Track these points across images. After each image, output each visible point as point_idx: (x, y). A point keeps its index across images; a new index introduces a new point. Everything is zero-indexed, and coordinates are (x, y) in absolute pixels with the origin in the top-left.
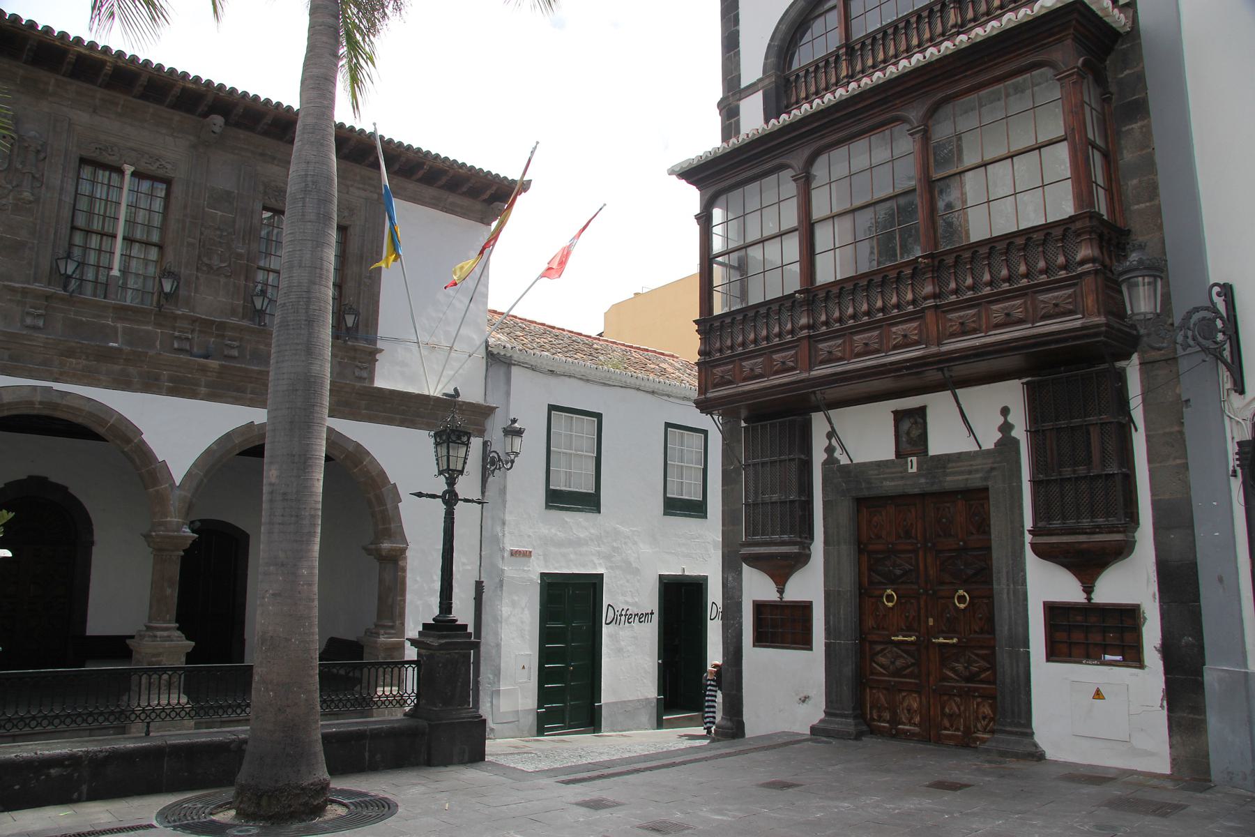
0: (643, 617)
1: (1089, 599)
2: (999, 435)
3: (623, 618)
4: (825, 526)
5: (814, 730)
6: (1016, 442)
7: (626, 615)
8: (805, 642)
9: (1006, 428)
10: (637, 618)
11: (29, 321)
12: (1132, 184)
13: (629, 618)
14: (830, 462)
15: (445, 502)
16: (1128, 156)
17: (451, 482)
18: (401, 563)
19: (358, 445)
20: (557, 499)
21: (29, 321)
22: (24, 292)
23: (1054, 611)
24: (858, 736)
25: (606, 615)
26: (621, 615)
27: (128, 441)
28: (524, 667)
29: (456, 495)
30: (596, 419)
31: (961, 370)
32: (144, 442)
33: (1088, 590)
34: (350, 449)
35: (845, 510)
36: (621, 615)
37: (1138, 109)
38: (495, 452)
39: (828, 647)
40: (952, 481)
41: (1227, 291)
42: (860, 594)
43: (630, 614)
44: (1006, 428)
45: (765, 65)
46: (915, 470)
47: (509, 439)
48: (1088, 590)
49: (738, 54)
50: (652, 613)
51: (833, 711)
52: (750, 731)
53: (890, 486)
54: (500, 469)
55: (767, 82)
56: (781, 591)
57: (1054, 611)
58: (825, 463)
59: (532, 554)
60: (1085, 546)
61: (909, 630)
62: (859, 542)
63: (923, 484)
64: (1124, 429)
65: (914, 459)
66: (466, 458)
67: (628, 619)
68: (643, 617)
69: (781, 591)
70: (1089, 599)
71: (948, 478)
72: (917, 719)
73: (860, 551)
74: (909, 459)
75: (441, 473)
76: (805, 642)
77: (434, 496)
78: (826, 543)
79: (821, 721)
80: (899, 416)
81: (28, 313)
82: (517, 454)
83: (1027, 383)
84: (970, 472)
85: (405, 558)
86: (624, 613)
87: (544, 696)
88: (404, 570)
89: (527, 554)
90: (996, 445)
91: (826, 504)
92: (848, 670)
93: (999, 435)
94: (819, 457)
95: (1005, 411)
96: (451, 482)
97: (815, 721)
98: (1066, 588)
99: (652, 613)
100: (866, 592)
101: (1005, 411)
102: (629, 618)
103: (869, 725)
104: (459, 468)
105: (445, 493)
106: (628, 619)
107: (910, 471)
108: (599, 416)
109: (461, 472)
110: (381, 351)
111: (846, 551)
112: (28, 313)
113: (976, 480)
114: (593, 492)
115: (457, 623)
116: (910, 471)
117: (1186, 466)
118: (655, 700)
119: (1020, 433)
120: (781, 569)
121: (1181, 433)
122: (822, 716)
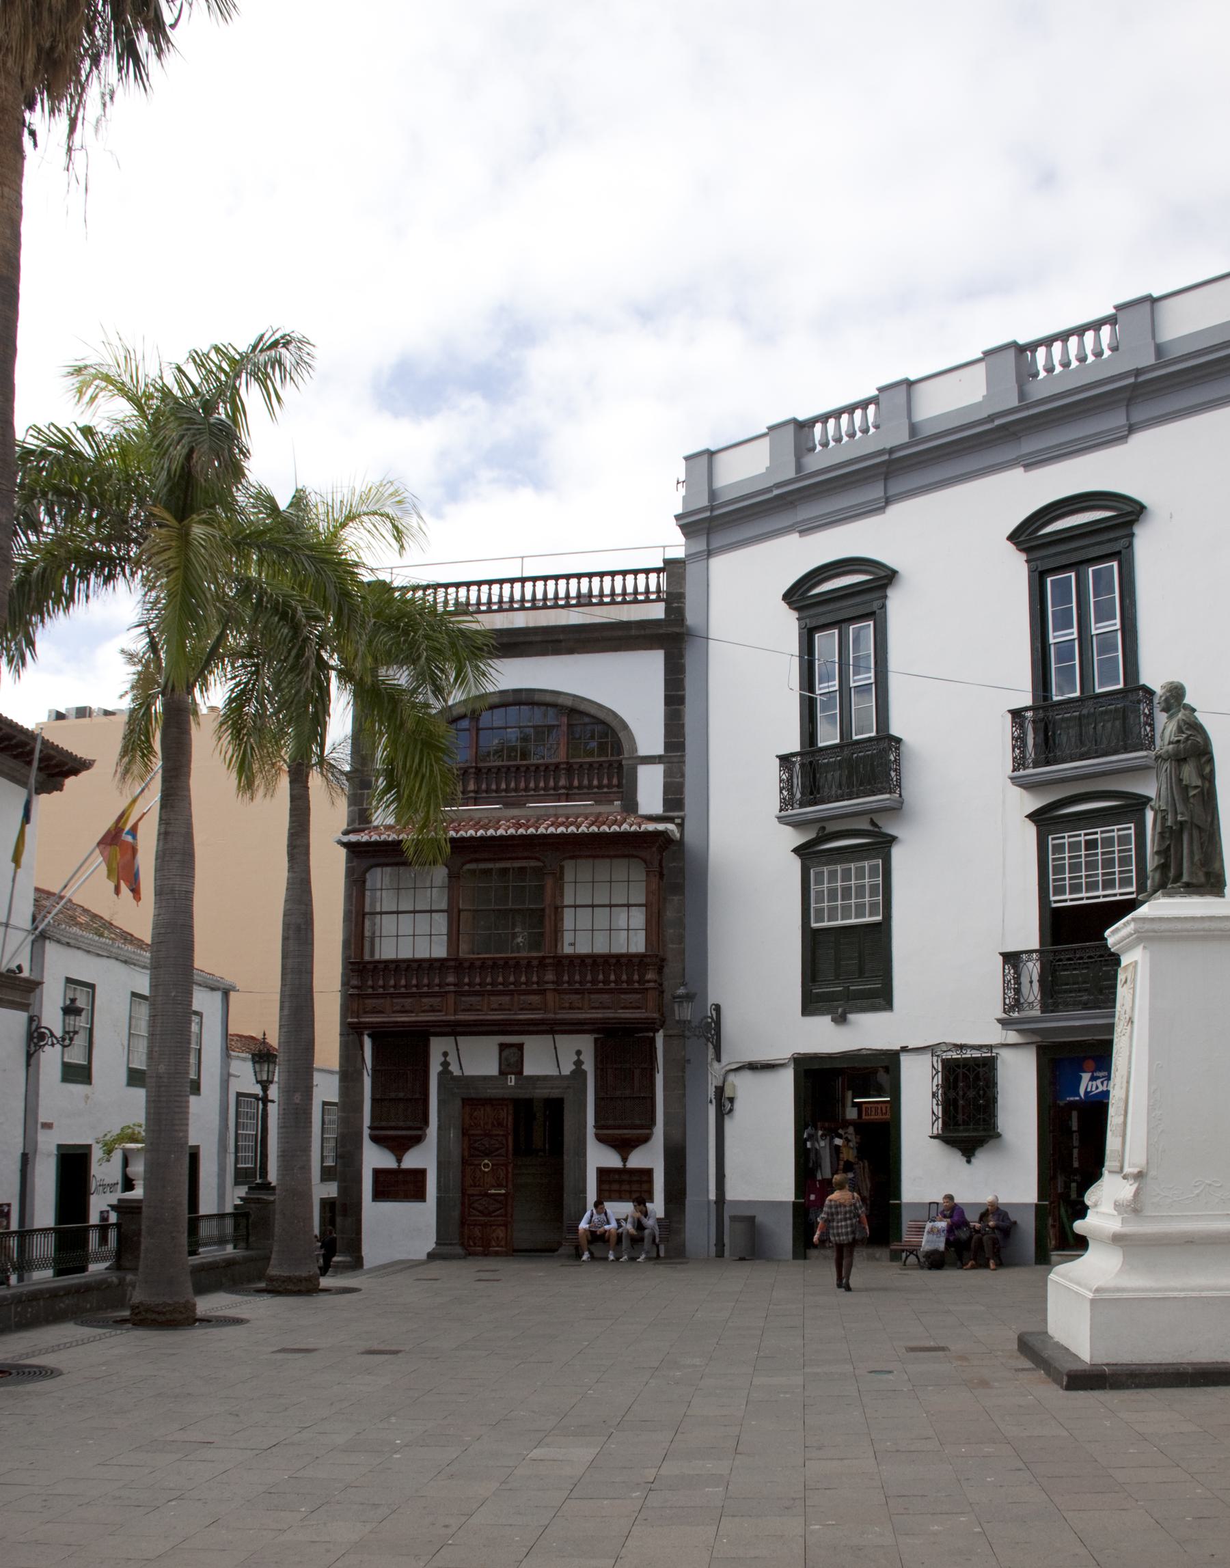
1: (625, 1165)
2: (574, 1067)
4: (439, 1117)
6: (584, 1073)
9: (579, 1063)
14: (445, 1072)
23: (603, 1173)
39: (440, 1202)
40: (541, 1092)
42: (463, 1163)
44: (579, 1063)
46: (513, 1084)
51: (442, 1242)
57: (603, 1173)
58: (440, 1074)
60: (627, 1136)
61: (499, 1186)
62: (463, 1129)
65: (513, 1077)
70: (625, 1165)
71: (537, 1091)
72: (503, 1243)
73: (464, 1134)
74: (509, 1076)
76: (420, 1196)
84: (552, 1088)
90: (571, 1072)
93: (574, 1067)
94: (435, 1069)
95: (579, 1053)
98: (612, 1160)
101: (579, 1053)
107: (509, 1084)
108: (92, 987)
113: (555, 1093)
116: (509, 1084)
117: (684, 1095)
119: (589, 1067)
120: (399, 1146)
121: (683, 1077)
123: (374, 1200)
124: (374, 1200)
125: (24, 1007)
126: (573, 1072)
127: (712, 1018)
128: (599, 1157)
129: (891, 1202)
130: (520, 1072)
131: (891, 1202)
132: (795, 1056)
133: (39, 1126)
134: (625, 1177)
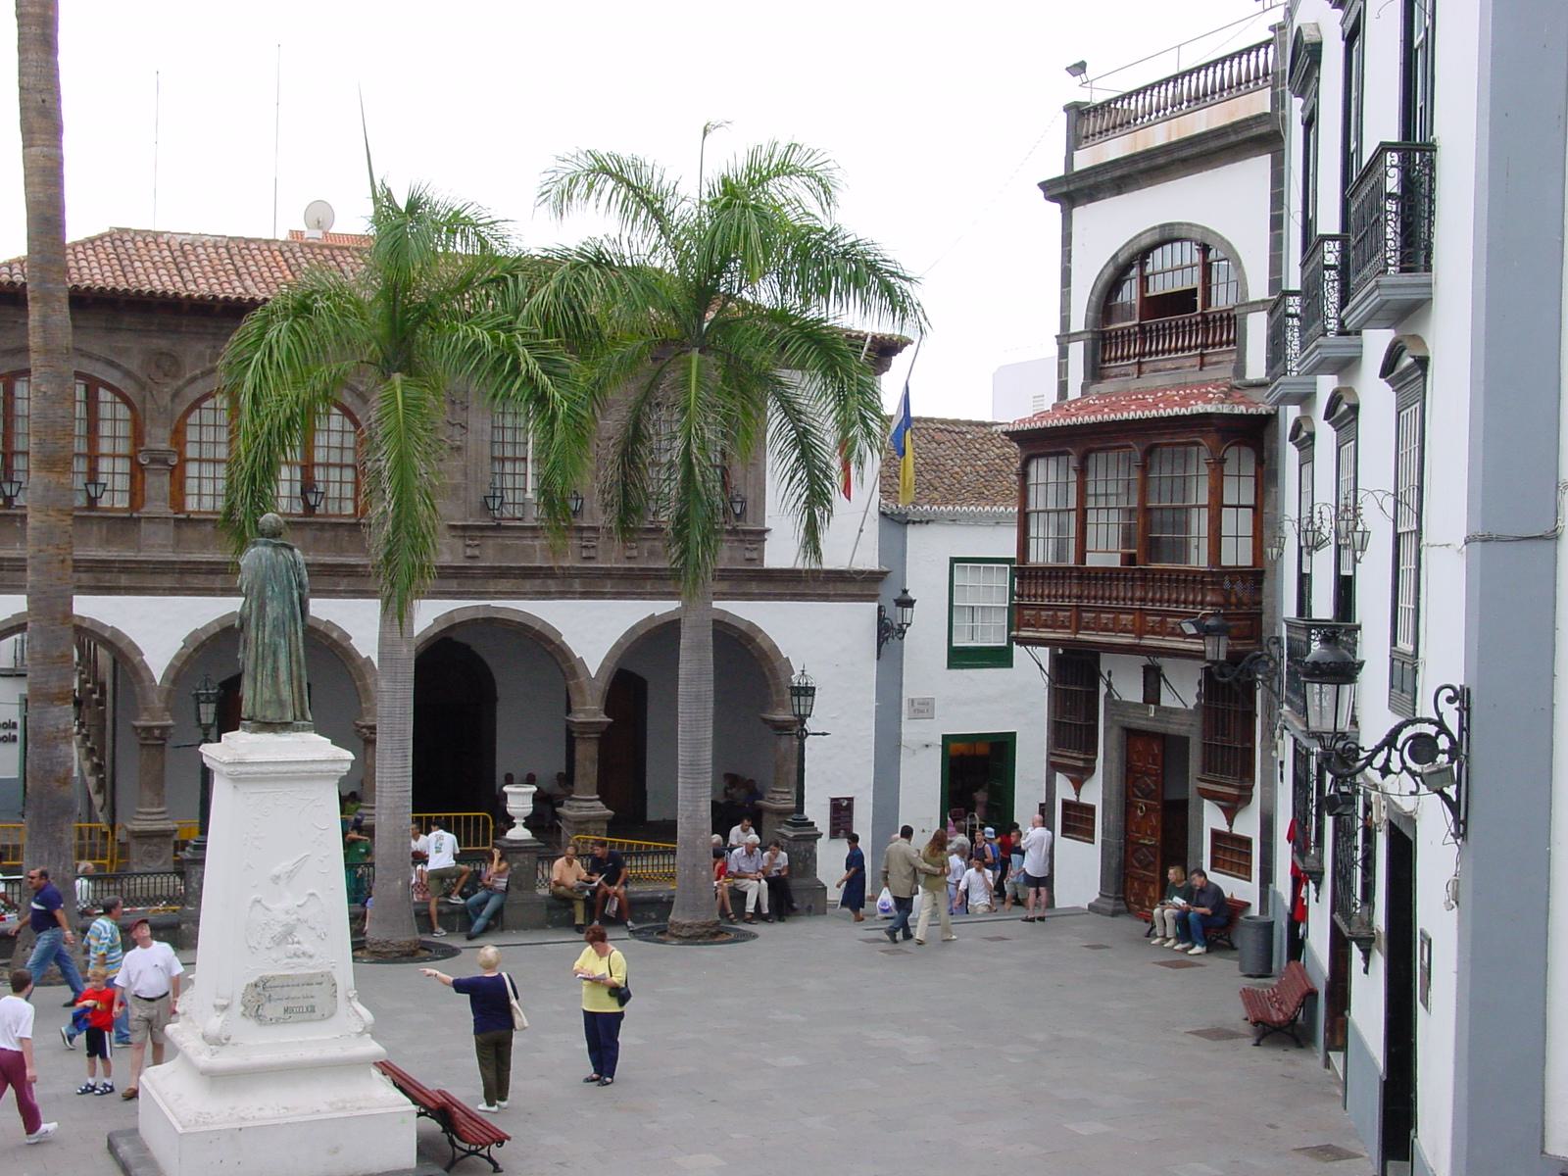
5: (1090, 906)
8: (1088, 835)
11: (469, 552)
14: (1109, 695)
19: (751, 624)
20: (961, 658)
21: (469, 552)
22: (465, 528)
24: (1115, 914)
27: (551, 642)
32: (563, 642)
33: (1230, 823)
34: (743, 628)
35: (1115, 732)
47: (899, 609)
48: (1230, 823)
49: (1069, 293)
52: (1057, 906)
55: (1085, 336)
57: (1216, 835)
63: (1160, 728)
64: (1251, 716)
79: (1097, 900)
81: (469, 546)
82: (909, 625)
84: (1181, 725)
92: (1114, 863)
97: (1093, 901)
100: (1128, 807)
103: (1127, 906)
110: (769, 530)
112: (469, 546)
122: (1098, 896)
125: (872, 598)
128: (1212, 818)
130: (1157, 702)
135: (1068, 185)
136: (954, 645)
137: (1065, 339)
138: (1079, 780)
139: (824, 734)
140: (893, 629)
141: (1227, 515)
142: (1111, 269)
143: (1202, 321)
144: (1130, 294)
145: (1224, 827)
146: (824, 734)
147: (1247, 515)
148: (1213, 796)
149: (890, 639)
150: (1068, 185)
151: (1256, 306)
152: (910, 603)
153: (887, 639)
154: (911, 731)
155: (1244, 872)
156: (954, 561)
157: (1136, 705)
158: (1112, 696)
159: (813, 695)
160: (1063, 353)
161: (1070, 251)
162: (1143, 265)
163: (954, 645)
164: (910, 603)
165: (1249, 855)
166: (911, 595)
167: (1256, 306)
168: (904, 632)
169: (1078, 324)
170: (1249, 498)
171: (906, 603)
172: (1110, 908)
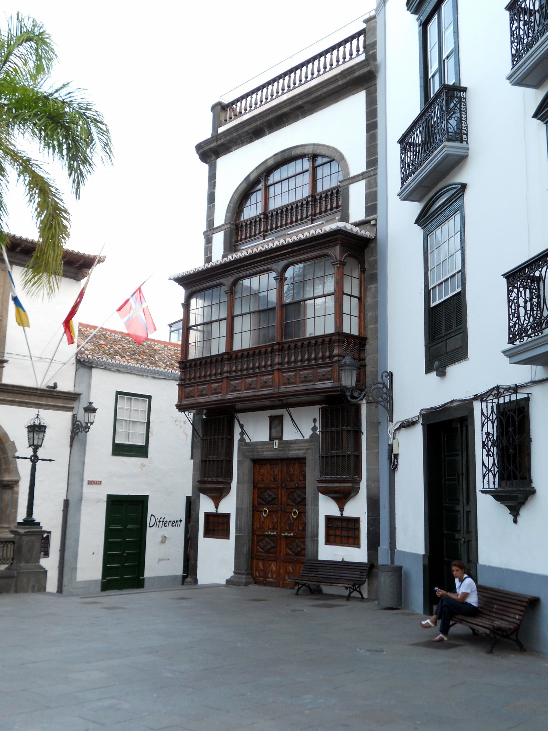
0: (174, 523)
1: (342, 514)
2: (312, 432)
3: (161, 523)
4: (238, 474)
5: (228, 581)
7: (163, 521)
8: (225, 535)
10: (170, 524)
12: (369, 314)
13: (165, 523)
14: (242, 440)
15: (32, 461)
16: (369, 301)
17: (35, 451)
18: (15, 489)
24: (247, 584)
25: (150, 521)
26: (160, 521)
28: (93, 553)
29: (37, 457)
30: (147, 400)
31: (292, 400)
33: (341, 509)
35: (248, 464)
36: (160, 521)
37: (374, 278)
38: (79, 421)
39: (237, 538)
40: (293, 453)
41: (391, 374)
42: (253, 510)
43: (167, 521)
45: (226, 216)
46: (277, 447)
47: (87, 414)
48: (341, 509)
49: (214, 206)
50: (181, 521)
51: (239, 572)
52: (200, 582)
53: (268, 454)
54: (81, 432)
55: (226, 227)
56: (217, 507)
57: (329, 519)
59: (102, 482)
60: (337, 489)
62: (254, 483)
63: (281, 455)
64: (358, 433)
65: (277, 441)
66: (43, 439)
67: (165, 524)
68: (174, 523)
69: (217, 507)
70: (342, 514)
71: (291, 452)
72: (275, 576)
73: (254, 487)
74: (275, 441)
75: (30, 446)
77: (26, 458)
78: (238, 482)
79: (232, 577)
80: (272, 419)
82: (92, 423)
83: (322, 408)
84: (299, 450)
85: (18, 486)
86: (162, 520)
87: (106, 571)
88: (17, 493)
89: (99, 483)
90: (310, 437)
91: (239, 462)
92: (245, 550)
93: (312, 432)
94: (237, 437)
96: (35, 451)
97: (229, 577)
99: (181, 521)
100: (255, 509)
101: (315, 420)
102: (165, 523)
103: (254, 579)
104: (40, 444)
105: (31, 457)
106: (165, 524)
108: (149, 397)
109: (40, 446)
110: (6, 361)
111: (247, 488)
113: (301, 454)
114: (144, 444)
115: (35, 522)
116: (275, 447)
118: (181, 577)
122: (233, 574)
123: (204, 537)
124: (204, 537)
125: (70, 409)
126: (311, 436)
127: (383, 384)
129: (141, 578)
130: (280, 438)
131: (141, 578)
132: (422, 412)
133: (85, 483)
134: (344, 524)
135: (217, 141)
136: (116, 442)
137: (211, 230)
138: (217, 498)
139: (50, 460)
140: (82, 426)
141: (346, 299)
142: (245, 185)
143: (312, 201)
144: (257, 198)
145: (336, 513)
146: (50, 460)
147: (355, 301)
148: (326, 492)
149: (80, 433)
150: (217, 141)
151: (356, 179)
152: (94, 410)
153: (77, 433)
154: (87, 490)
155: (357, 544)
156: (118, 393)
157: (263, 443)
158: (244, 440)
159: (44, 432)
160: (209, 241)
161: (215, 183)
162: (266, 180)
163: (116, 442)
164: (94, 410)
165: (358, 529)
166: (94, 405)
167: (356, 179)
168: (89, 428)
169: (220, 219)
170: (356, 293)
171: (90, 409)
172: (244, 580)
